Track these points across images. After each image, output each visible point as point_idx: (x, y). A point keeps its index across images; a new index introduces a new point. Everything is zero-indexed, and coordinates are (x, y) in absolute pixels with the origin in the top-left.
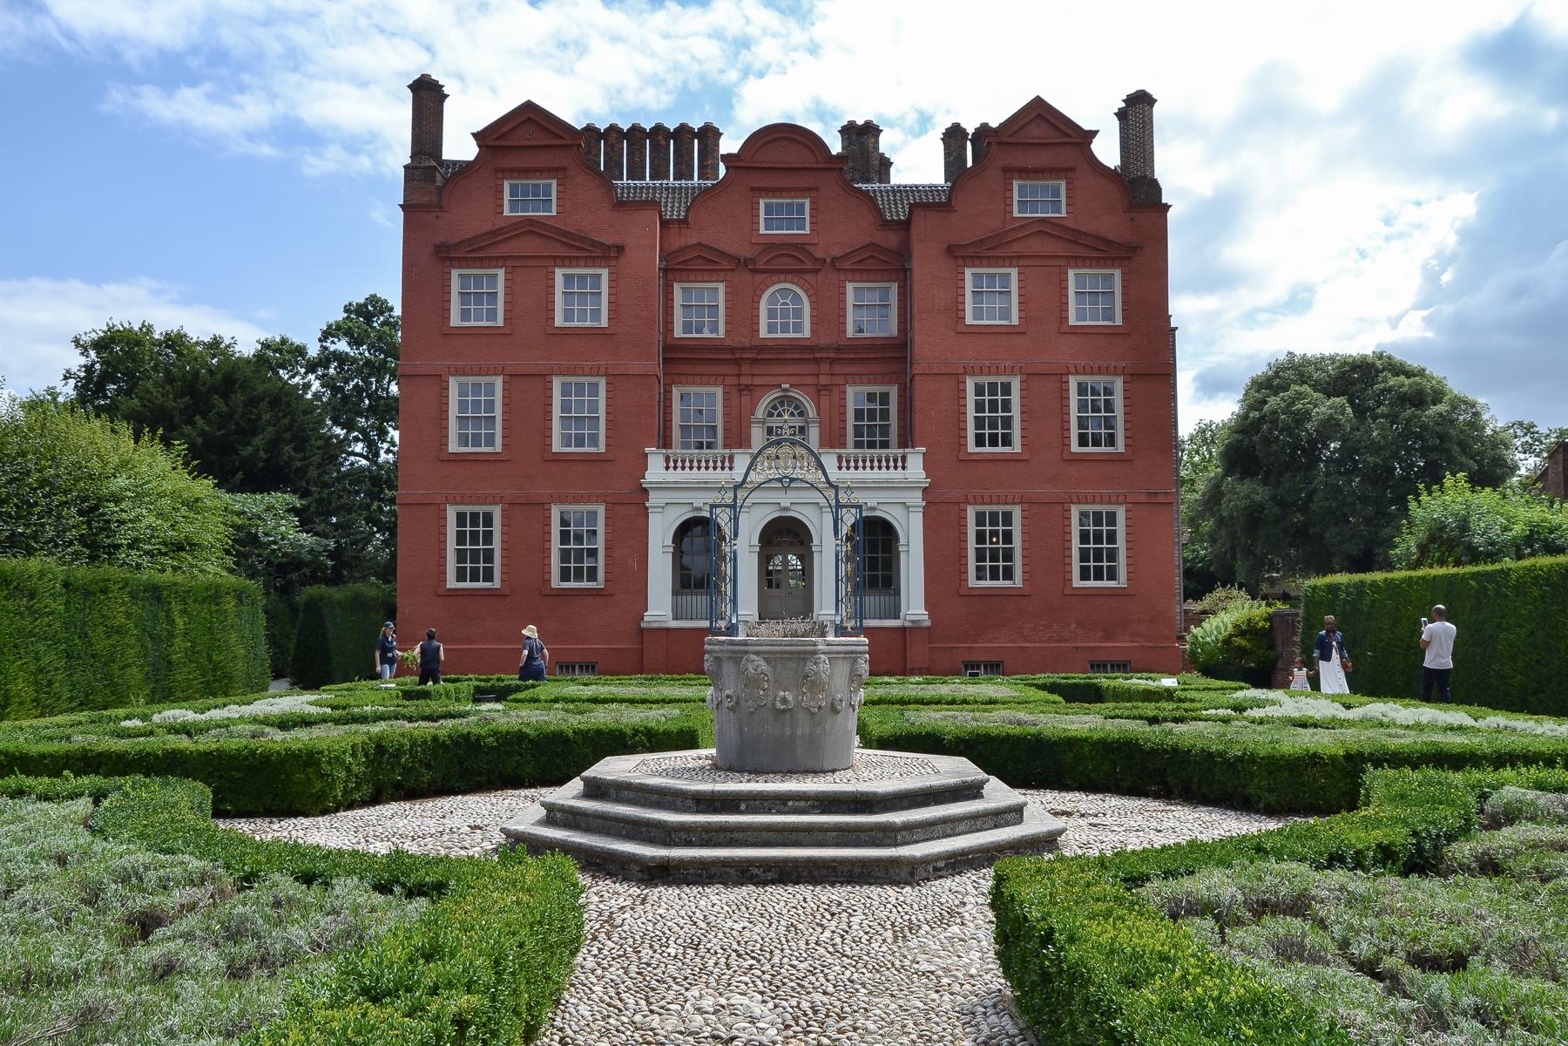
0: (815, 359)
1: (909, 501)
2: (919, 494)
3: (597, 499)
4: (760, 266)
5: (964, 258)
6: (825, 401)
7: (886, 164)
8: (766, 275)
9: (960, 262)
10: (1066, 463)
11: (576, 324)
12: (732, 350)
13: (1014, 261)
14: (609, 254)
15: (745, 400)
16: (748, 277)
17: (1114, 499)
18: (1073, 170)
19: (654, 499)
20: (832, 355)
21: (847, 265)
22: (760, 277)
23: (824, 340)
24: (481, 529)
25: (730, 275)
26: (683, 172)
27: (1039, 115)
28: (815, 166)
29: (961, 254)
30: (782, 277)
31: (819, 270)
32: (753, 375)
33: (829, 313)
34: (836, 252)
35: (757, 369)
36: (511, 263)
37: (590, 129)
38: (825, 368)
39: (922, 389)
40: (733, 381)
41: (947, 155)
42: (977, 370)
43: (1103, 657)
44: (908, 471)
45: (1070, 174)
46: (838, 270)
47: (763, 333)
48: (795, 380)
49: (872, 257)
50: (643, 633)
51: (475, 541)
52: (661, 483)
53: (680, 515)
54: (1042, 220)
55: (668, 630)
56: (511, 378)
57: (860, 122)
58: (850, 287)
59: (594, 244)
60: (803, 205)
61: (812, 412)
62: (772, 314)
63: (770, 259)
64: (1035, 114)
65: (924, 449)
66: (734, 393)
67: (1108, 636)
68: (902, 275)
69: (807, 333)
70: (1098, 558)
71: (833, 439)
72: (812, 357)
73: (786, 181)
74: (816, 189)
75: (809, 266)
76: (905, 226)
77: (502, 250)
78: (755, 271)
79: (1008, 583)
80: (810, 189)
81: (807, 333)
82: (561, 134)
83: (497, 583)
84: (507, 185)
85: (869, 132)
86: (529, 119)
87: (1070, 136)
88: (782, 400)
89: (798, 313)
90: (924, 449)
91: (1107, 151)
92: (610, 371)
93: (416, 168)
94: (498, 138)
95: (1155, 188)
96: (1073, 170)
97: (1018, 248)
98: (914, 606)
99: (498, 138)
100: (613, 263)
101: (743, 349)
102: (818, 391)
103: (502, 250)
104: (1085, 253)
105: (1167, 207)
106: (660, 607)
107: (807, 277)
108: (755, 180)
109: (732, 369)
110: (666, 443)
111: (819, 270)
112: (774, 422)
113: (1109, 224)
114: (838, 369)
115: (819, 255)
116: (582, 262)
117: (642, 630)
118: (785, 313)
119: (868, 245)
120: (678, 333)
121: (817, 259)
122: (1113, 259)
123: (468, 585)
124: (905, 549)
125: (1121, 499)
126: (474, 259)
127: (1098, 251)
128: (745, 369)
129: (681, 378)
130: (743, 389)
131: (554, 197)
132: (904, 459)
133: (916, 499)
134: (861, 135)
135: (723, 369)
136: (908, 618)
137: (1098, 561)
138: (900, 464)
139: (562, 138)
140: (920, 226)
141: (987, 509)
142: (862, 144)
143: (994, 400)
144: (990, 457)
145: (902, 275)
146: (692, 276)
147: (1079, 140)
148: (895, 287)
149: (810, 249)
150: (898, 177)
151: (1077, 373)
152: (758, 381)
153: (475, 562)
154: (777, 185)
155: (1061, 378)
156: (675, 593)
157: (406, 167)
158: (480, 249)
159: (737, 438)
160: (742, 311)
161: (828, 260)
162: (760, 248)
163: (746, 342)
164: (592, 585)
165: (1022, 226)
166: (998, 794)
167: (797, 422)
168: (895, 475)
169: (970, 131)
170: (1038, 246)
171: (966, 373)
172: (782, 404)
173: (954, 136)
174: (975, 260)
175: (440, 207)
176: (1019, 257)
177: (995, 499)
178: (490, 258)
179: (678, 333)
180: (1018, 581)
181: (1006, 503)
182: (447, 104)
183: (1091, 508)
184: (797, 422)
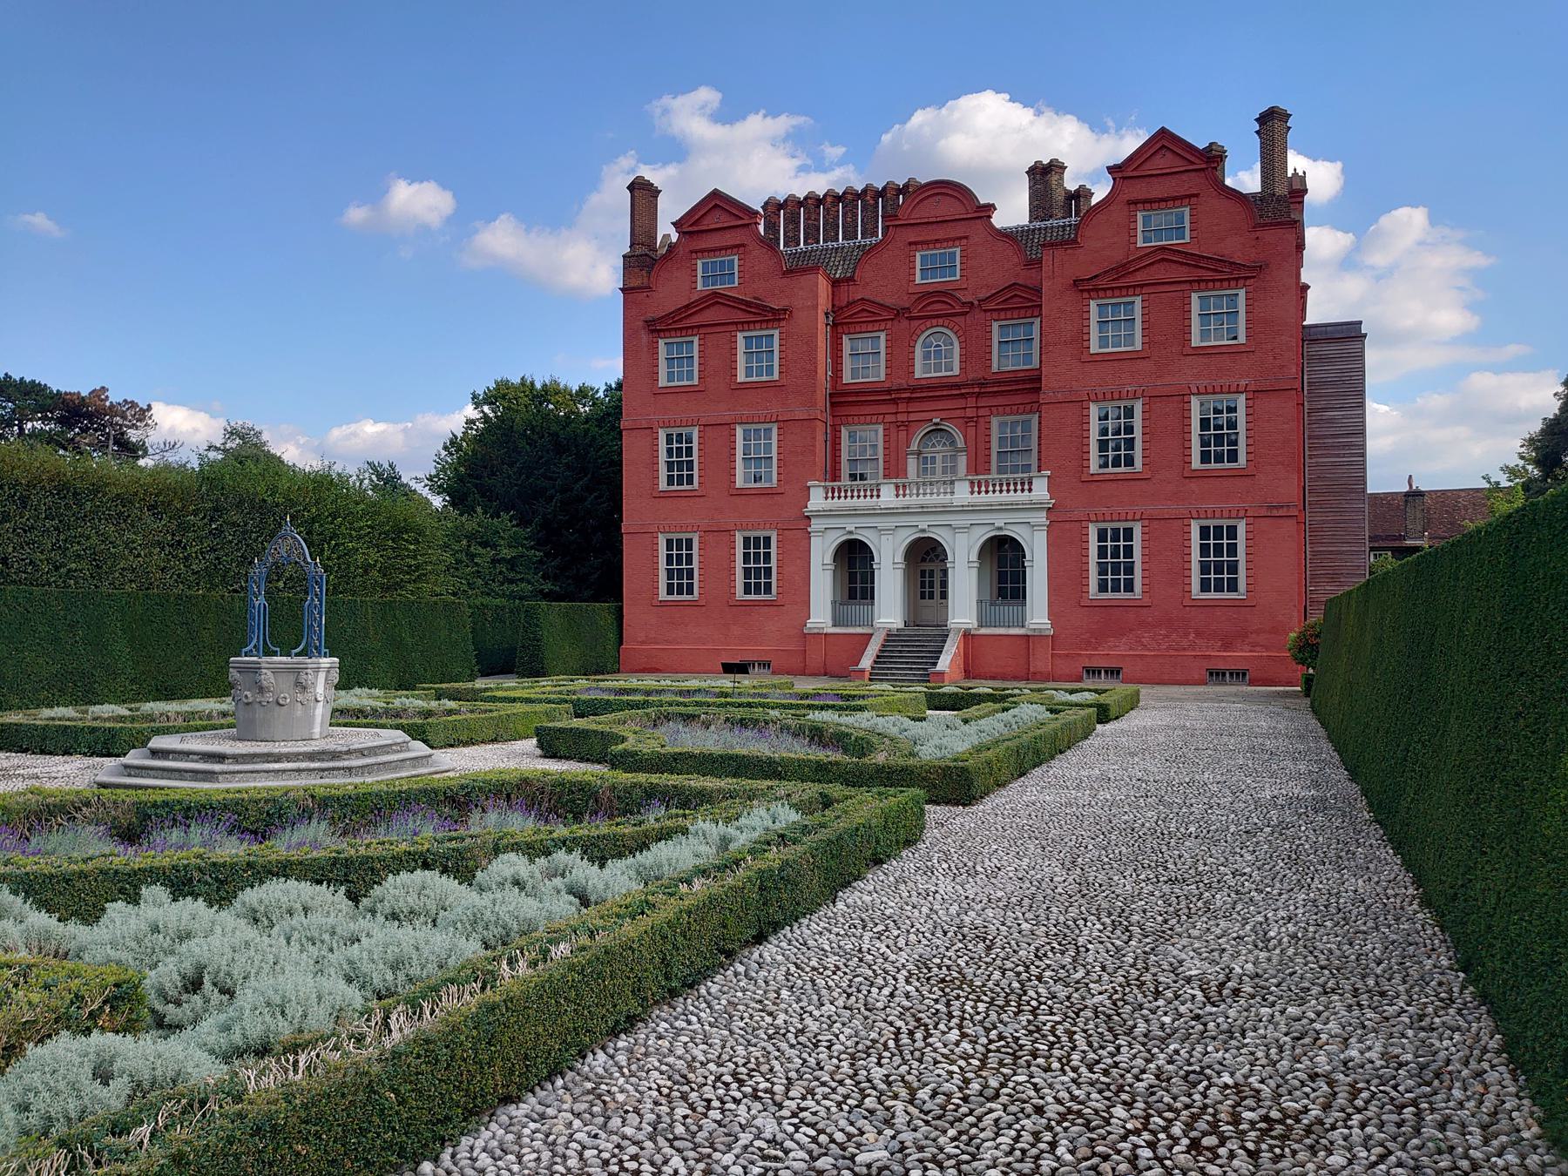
0: (962, 394)
2: (1044, 514)
5: (1088, 291)
8: (921, 321)
9: (1086, 295)
10: (1188, 480)
11: (755, 379)
12: (889, 392)
13: (1138, 291)
15: (903, 434)
16: (905, 323)
17: (1234, 513)
18: (1196, 195)
19: (816, 524)
20: (977, 390)
21: (992, 306)
22: (916, 323)
24: (684, 552)
25: (889, 324)
26: (850, 234)
27: (1163, 146)
28: (965, 216)
29: (1086, 288)
30: (934, 322)
31: (968, 312)
32: (909, 412)
34: (983, 294)
35: (914, 407)
36: (702, 331)
38: (971, 402)
42: (1100, 396)
43: (1221, 666)
44: (1033, 493)
45: (1194, 200)
46: (985, 311)
49: (1016, 296)
50: (807, 638)
51: (757, 561)
52: (819, 511)
53: (835, 539)
54: (1163, 248)
57: (1046, 162)
58: (995, 325)
59: (764, 308)
61: (960, 443)
63: (924, 307)
64: (1158, 146)
66: (893, 429)
67: (1227, 646)
69: (956, 371)
70: (1219, 570)
72: (958, 392)
73: (940, 233)
74: (966, 237)
75: (958, 310)
78: (910, 319)
79: (1128, 595)
80: (960, 238)
82: (741, 215)
84: (699, 263)
85: (1052, 170)
86: (716, 206)
87: (1192, 163)
89: (949, 353)
92: (780, 418)
93: (633, 256)
94: (691, 226)
96: (1196, 195)
97: (1140, 277)
98: (1037, 613)
99: (691, 226)
100: (783, 323)
101: (898, 390)
102: (966, 422)
106: (820, 616)
111: (968, 312)
113: (1235, 248)
120: (847, 378)
121: (963, 303)
123: (675, 597)
124: (1030, 564)
125: (1242, 513)
128: (902, 407)
129: (847, 419)
130: (900, 425)
132: (1030, 483)
133: (1041, 518)
135: (883, 409)
136: (1032, 627)
137: (1219, 572)
138: (1026, 487)
141: (1109, 526)
144: (1112, 477)
147: (1204, 166)
151: (1199, 393)
152: (913, 417)
153: (680, 579)
154: (952, 235)
157: (624, 256)
158: (680, 320)
159: (894, 470)
160: (900, 357)
161: (976, 303)
164: (767, 597)
165: (1145, 255)
166: (419, 748)
168: (1021, 497)
170: (1160, 273)
174: (1096, 292)
176: (1142, 286)
177: (1234, 513)
181: (1126, 520)
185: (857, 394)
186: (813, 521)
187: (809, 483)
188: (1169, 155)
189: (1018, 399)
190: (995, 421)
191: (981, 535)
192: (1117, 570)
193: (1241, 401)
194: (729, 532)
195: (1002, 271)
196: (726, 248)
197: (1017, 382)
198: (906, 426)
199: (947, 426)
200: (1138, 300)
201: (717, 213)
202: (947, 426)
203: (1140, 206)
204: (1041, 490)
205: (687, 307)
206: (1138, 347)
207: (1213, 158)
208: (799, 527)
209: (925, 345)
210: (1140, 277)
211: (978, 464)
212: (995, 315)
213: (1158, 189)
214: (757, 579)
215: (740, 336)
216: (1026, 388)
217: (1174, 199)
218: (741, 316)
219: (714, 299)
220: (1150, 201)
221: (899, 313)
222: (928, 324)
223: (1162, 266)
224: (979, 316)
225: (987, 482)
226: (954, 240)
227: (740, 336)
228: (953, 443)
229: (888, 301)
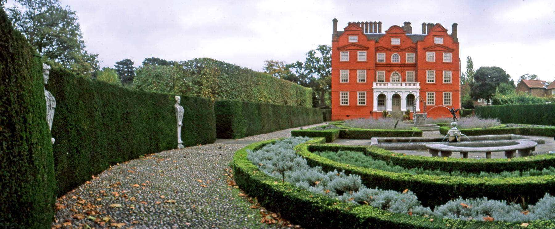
7: (411, 28)
14: (367, 49)
19: (374, 91)
22: (391, 52)
29: (426, 49)
33: (403, 58)
35: (391, 68)
37: (359, 23)
38: (402, 68)
39: (420, 72)
47: (392, 62)
53: (378, 93)
55: (377, 113)
56: (351, 70)
57: (407, 22)
58: (407, 54)
61: (400, 76)
62: (393, 58)
68: (416, 52)
69: (399, 62)
71: (404, 80)
76: (417, 43)
81: (399, 62)
83: (348, 105)
88: (395, 73)
89: (398, 58)
91: (450, 32)
97: (436, 49)
102: (401, 72)
106: (376, 108)
108: (391, 35)
109: (387, 68)
110: (375, 81)
112: (394, 77)
114: (406, 68)
115: (401, 48)
118: (396, 58)
127: (447, 49)
128: (389, 68)
130: (388, 71)
133: (418, 91)
134: (407, 24)
140: (419, 43)
145: (416, 52)
148: (414, 54)
150: (414, 32)
167: (398, 77)
169: (427, 24)
179: (377, 62)
182: (338, 23)
183: (446, 93)
184: (398, 77)
189: (411, 68)
190: (407, 72)
191: (407, 94)
192: (431, 101)
194: (356, 92)
195: (409, 44)
198: (390, 71)
199: (397, 72)
204: (418, 86)
206: (435, 61)
208: (371, 91)
209: (393, 56)
210: (436, 49)
216: (414, 66)
218: (358, 48)
224: (404, 52)
228: (399, 75)
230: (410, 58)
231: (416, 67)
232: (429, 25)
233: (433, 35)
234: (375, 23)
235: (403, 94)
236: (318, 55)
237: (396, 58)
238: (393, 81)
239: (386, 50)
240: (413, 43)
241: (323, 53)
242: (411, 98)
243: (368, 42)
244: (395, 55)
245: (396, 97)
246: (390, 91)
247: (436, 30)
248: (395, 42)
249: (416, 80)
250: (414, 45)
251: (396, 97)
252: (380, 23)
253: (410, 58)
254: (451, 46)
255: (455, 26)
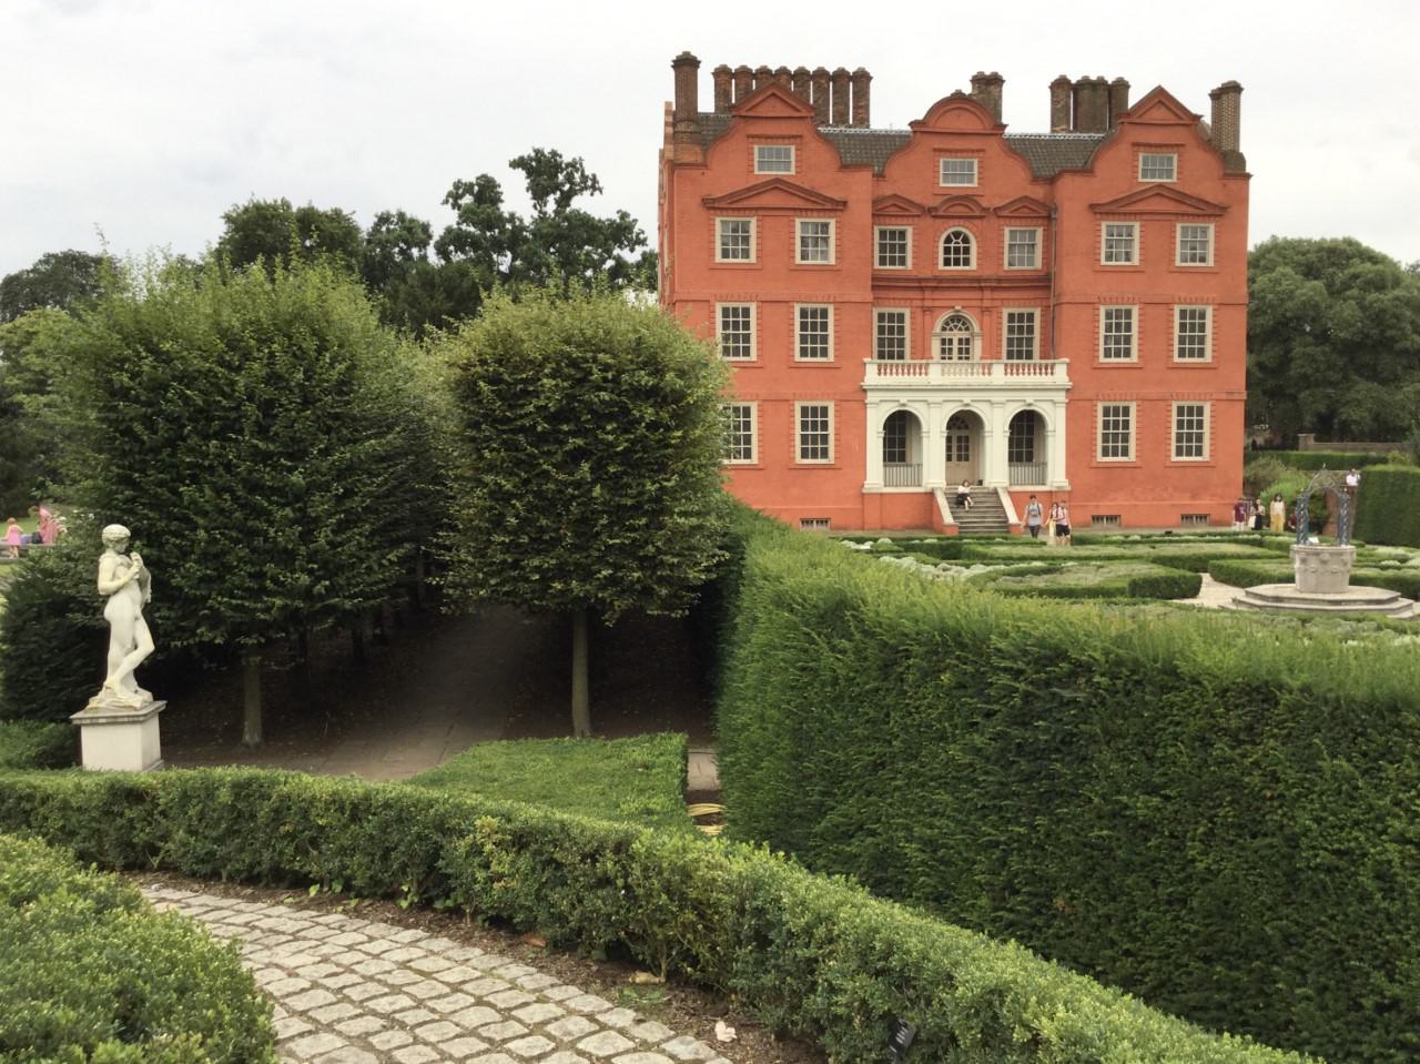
1: (1056, 399)
2: (1063, 394)
3: (828, 397)
4: (940, 213)
6: (986, 319)
12: (920, 280)
14: (839, 206)
15: (928, 317)
16: (929, 221)
18: (1183, 145)
19: (871, 397)
21: (1006, 213)
22: (939, 221)
23: (988, 272)
30: (956, 222)
35: (937, 295)
36: (760, 213)
38: (987, 294)
39: (1067, 314)
40: (919, 303)
41: (1054, 102)
48: (964, 303)
50: (863, 497)
54: (1160, 185)
55: (881, 494)
57: (988, 73)
58: (1007, 230)
59: (826, 199)
60: (972, 163)
61: (976, 328)
62: (947, 251)
65: (1067, 360)
67: (1194, 496)
70: (1189, 440)
71: (991, 353)
74: (983, 151)
75: (978, 214)
77: (755, 202)
78: (935, 217)
80: (978, 151)
82: (799, 107)
83: (755, 459)
88: (952, 319)
89: (967, 251)
90: (1067, 360)
95: (1241, 160)
98: (1057, 473)
99: (750, 109)
100: (839, 213)
101: (927, 280)
102: (984, 310)
103: (755, 202)
104: (1191, 210)
105: (1248, 176)
107: (976, 222)
108: (937, 143)
109: (918, 295)
112: (947, 335)
114: (997, 295)
115: (985, 205)
116: (815, 214)
117: (863, 494)
118: (957, 251)
119: (1020, 200)
122: (1209, 216)
126: (733, 209)
128: (928, 294)
130: (925, 310)
131: (793, 159)
133: (1061, 397)
135: (910, 294)
139: (798, 111)
142: (989, 93)
143: (1119, 323)
146: (887, 220)
148: (1040, 233)
149: (978, 199)
152: (937, 303)
155: (1168, 305)
156: (885, 466)
162: (939, 200)
163: (927, 273)
164: (824, 461)
167: (964, 335)
171: (1099, 303)
172: (953, 321)
173: (1060, 85)
175: (704, 165)
176: (1141, 214)
178: (745, 209)
180: (1132, 456)
184: (964, 335)
185: (888, 279)
186: (869, 394)
187: (866, 360)
188: (1163, 110)
189: (1026, 294)
193: (1209, 312)
195: (1013, 183)
196: (783, 137)
197: (1027, 280)
200: (1137, 227)
201: (772, 101)
202: (966, 314)
203: (1142, 148)
204: (1061, 375)
205: (749, 189)
207: (1197, 118)
209: (948, 240)
211: (991, 353)
212: (1007, 221)
213: (1155, 136)
214: (814, 445)
215: (798, 222)
216: (1042, 284)
217: (1167, 146)
219: (777, 185)
220: (1150, 145)
221: (931, 212)
222: (951, 222)
223: (1157, 199)
224: (994, 222)
225: (1029, 365)
226: (973, 151)
227: (798, 222)
229: (917, 199)
230: (1016, 249)
231: (1048, 288)
232: (1085, 83)
233: (1136, 145)
234: (841, 75)
235: (998, 411)
236: (517, 201)
237: (957, 251)
238: (946, 352)
239: (915, 212)
240: (1035, 180)
241: (539, 194)
242: (1027, 429)
243: (840, 174)
244: (957, 235)
245: (964, 429)
246: (939, 397)
247: (1146, 119)
248: (956, 176)
249: (1050, 351)
250: (1038, 192)
251: (964, 429)
252: (862, 78)
253: (1016, 249)
254: (1209, 190)
255: (1227, 95)
